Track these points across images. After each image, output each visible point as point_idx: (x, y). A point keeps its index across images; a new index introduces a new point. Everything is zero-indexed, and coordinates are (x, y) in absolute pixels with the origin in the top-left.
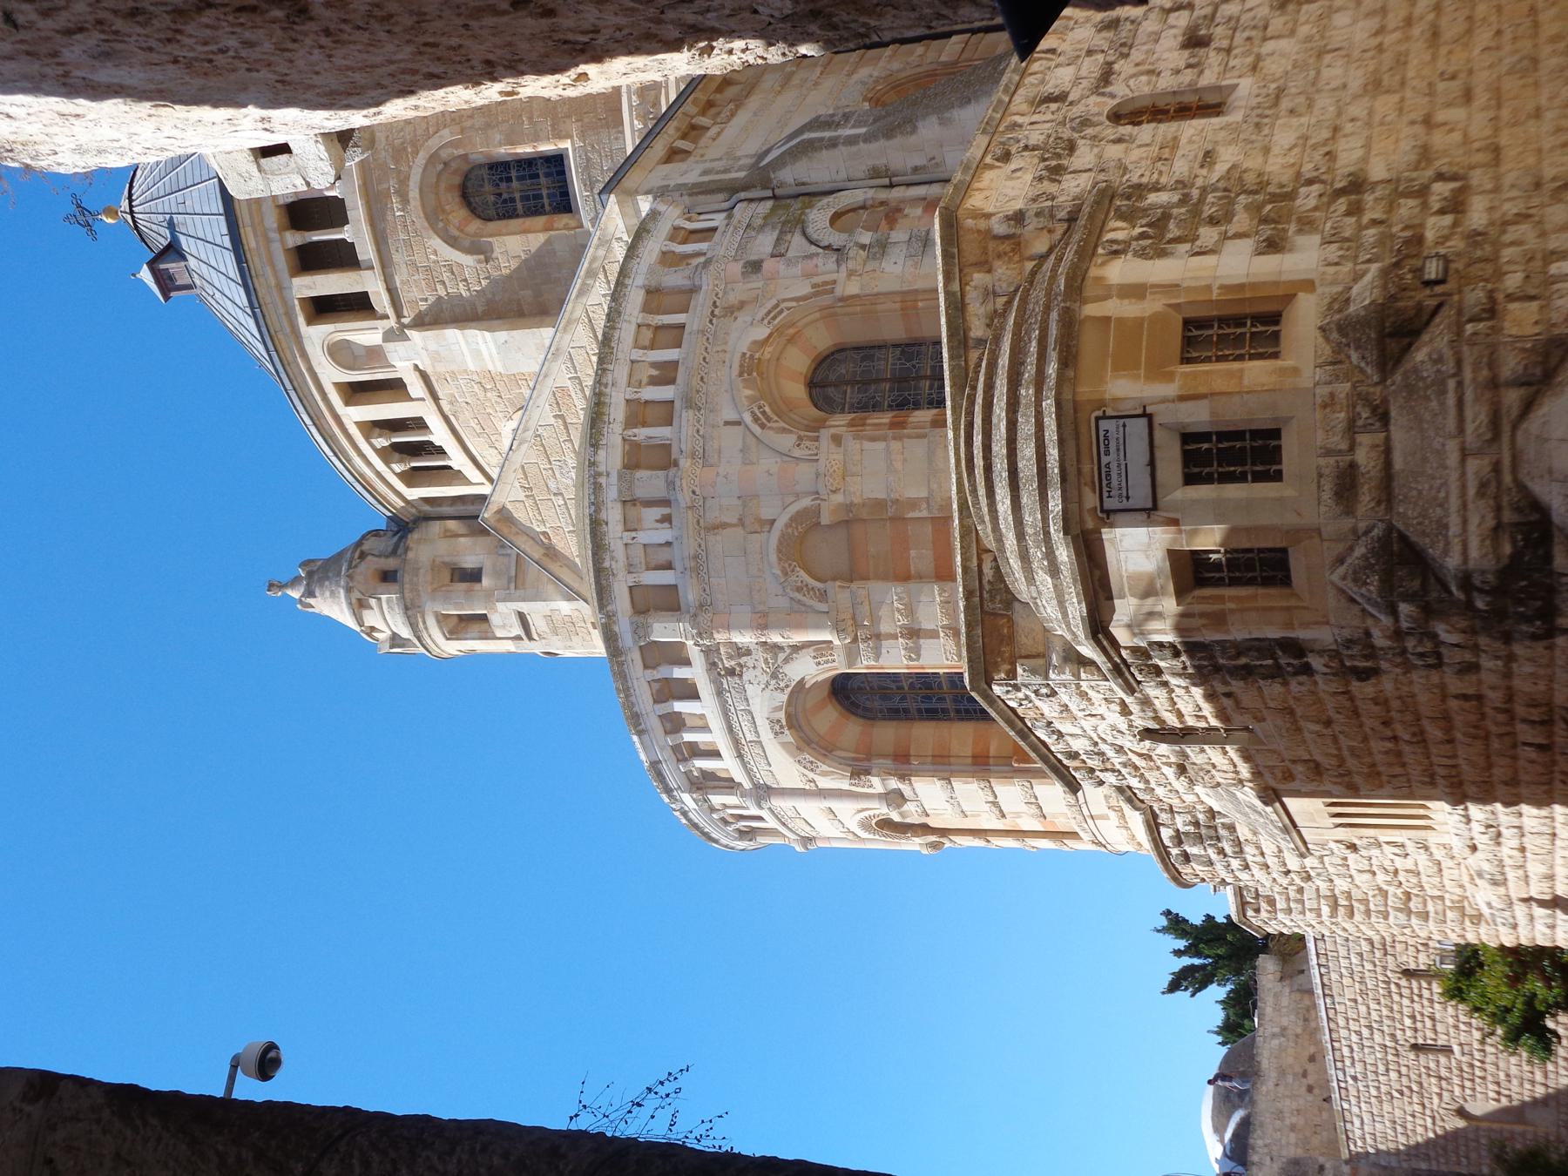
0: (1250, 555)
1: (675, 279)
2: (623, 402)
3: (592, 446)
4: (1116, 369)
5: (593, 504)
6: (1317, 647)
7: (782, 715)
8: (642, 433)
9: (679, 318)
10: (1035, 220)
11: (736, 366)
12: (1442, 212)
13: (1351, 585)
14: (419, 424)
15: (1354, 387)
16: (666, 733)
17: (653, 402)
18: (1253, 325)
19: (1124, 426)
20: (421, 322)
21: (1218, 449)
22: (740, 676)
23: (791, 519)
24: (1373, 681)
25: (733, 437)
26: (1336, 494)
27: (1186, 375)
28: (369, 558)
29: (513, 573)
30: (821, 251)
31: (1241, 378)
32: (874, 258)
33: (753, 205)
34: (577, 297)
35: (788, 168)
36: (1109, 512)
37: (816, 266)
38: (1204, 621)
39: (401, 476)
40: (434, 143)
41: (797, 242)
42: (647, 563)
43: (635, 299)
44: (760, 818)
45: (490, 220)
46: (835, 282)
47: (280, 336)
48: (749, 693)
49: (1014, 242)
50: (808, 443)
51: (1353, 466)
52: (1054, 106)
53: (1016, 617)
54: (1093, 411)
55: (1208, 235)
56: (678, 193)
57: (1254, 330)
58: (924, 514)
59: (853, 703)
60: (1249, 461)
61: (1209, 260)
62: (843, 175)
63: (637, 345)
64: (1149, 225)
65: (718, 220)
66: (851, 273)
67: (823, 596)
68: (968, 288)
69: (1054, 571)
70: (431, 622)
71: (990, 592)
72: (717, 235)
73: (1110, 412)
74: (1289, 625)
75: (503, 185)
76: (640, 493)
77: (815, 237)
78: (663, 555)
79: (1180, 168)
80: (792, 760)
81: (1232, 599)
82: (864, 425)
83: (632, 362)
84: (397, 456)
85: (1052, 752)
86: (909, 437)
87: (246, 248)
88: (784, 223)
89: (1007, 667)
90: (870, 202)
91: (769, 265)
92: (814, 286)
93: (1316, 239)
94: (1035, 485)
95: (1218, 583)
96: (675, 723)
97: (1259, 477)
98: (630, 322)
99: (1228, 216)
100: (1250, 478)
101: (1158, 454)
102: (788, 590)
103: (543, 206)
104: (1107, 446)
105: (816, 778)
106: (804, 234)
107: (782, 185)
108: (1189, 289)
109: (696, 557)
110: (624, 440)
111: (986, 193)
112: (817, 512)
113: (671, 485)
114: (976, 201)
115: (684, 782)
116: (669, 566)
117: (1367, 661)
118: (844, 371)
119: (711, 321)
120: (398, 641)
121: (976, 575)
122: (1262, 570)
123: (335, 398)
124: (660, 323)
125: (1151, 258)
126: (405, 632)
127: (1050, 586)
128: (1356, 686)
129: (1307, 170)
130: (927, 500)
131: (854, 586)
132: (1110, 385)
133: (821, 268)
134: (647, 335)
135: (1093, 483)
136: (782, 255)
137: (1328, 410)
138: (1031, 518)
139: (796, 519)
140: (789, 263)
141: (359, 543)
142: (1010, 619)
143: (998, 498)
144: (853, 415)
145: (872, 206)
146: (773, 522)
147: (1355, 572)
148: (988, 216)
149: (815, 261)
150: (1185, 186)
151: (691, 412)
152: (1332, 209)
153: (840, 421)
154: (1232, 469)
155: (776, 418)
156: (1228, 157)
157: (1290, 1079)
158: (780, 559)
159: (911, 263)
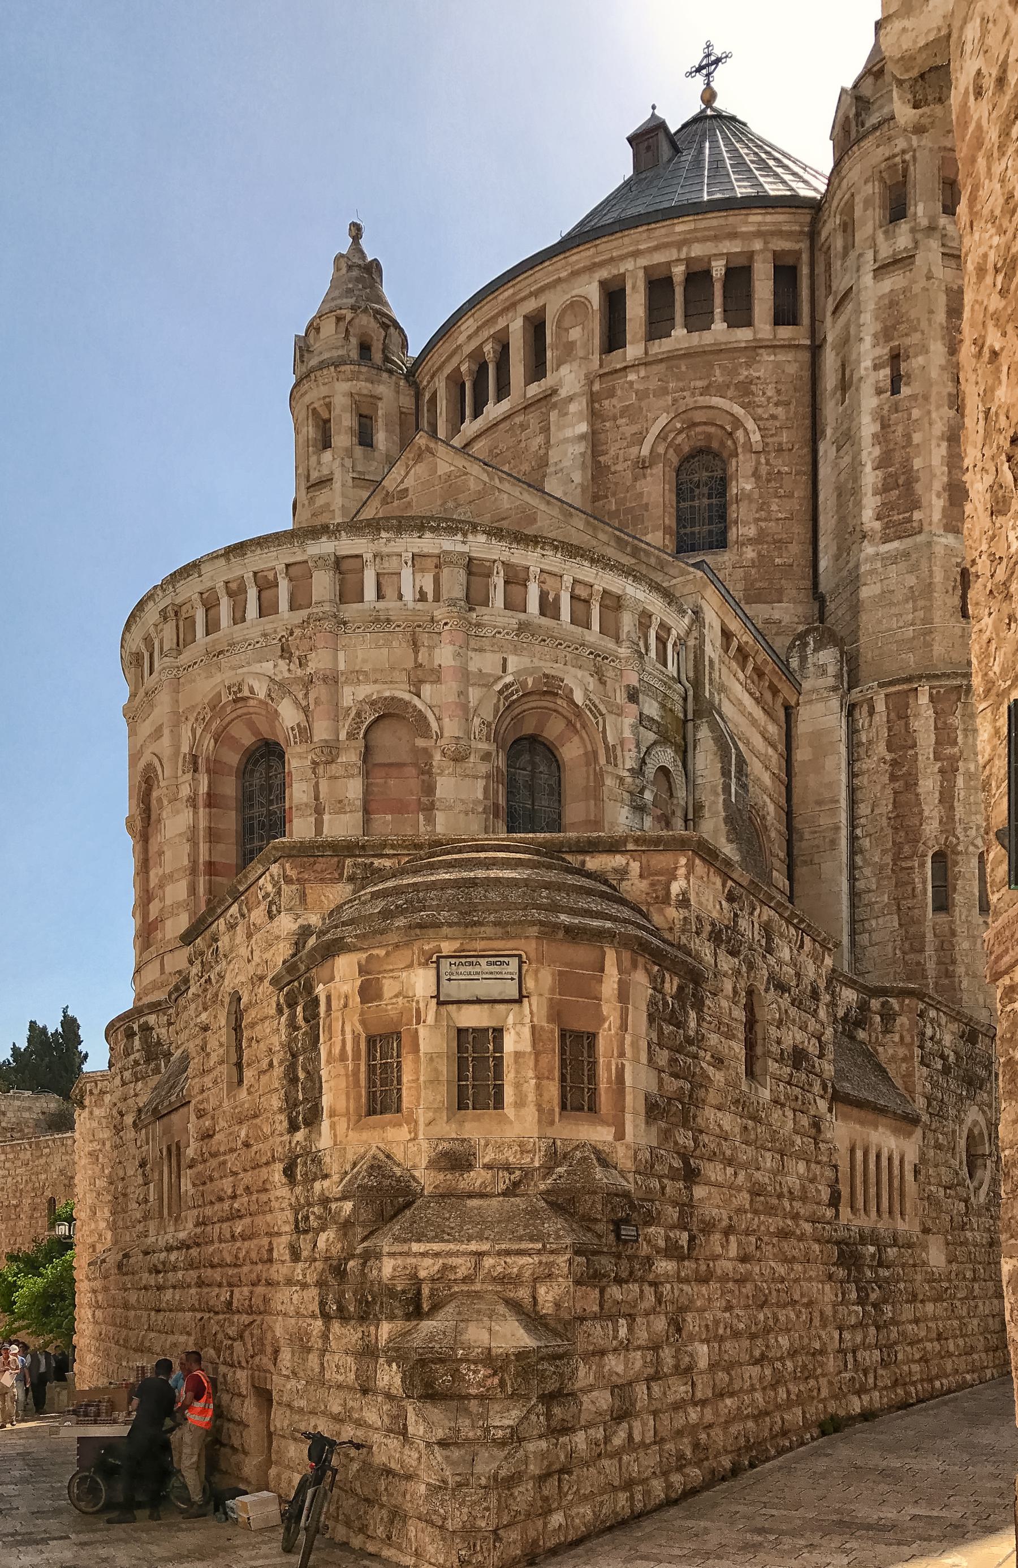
1: (628, 621)
7: (246, 693)
9: (596, 626)
11: (553, 672)
12: (667, 1238)
20: (593, 398)
22: (281, 657)
24: (284, 1180)
40: (750, 425)
48: (265, 664)
52: (763, 942)
73: (525, 967)
79: (713, 1039)
101: (486, 1006)
104: (495, 963)
119: (591, 653)
128: (279, 1167)
129: (705, 1138)
150: (699, 1041)
156: (718, 1077)
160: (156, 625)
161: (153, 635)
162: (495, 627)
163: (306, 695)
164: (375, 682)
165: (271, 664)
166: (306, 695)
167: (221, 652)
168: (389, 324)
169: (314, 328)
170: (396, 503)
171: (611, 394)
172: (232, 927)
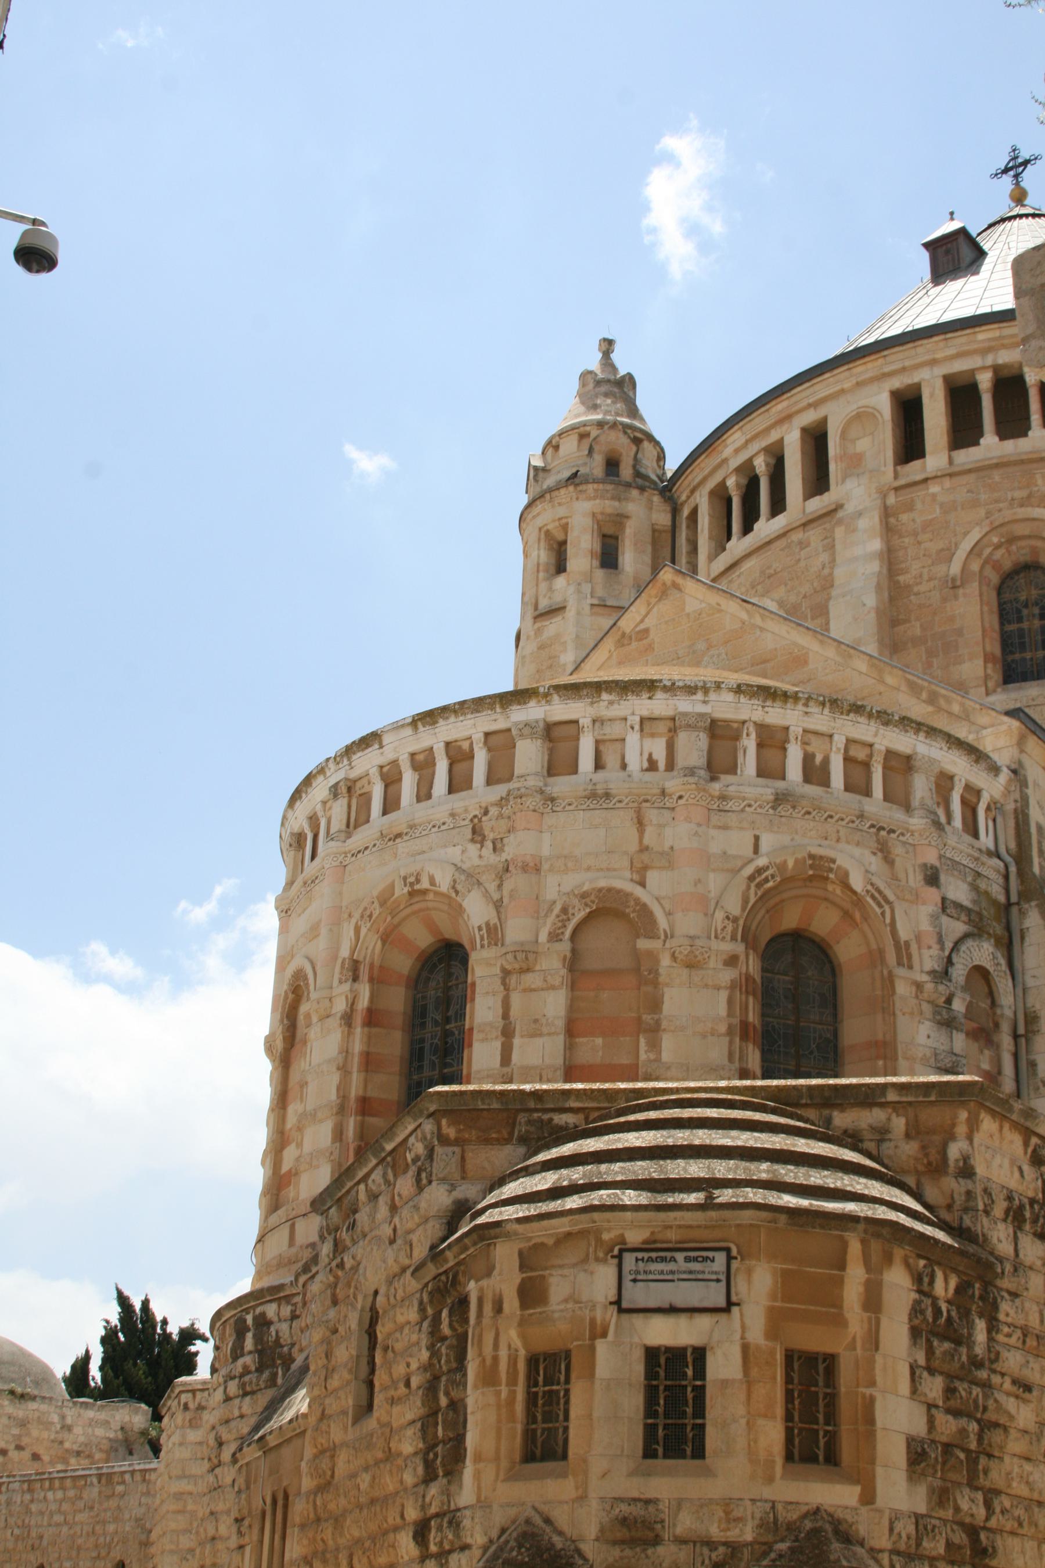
0: (561, 1417)
1: (921, 787)
2: (786, 723)
3: (739, 686)
4: (786, 1274)
5: (673, 684)
6: (453, 1488)
7: (425, 884)
8: (749, 743)
10: (963, 1190)
13: (520, 1530)
14: (778, 506)
15: (746, 1544)
16: (413, 755)
17: (785, 757)
18: (826, 1432)
19: (718, 1281)
20: (887, 513)
21: (686, 1386)
22: (473, 840)
23: (645, 905)
25: (738, 843)
26: (625, 1519)
27: (772, 1353)
28: (634, 448)
29: (609, 603)
30: (947, 953)
31: (765, 1416)
32: (936, 1013)
33: (1001, 881)
34: (908, 681)
36: (620, 1257)
37: (930, 947)
38: (489, 1362)
39: (722, 485)
41: (957, 927)
42: (604, 741)
43: (902, 742)
44: (313, 856)
45: (999, 594)
46: (910, 967)
47: (881, 361)
49: (938, 1168)
50: (730, 928)
51: (657, 1541)
53: (508, 1149)
54: (738, 1246)
55: (934, 1387)
56: (1017, 796)
57: (821, 1433)
58: (643, 1056)
59: (435, 966)
60: (670, 1421)
61: (905, 1387)
62: (1030, 982)
63: (850, 742)
64: (949, 1318)
65: (986, 840)
66: (919, 986)
67: (555, 937)
68: (890, 1110)
69: (556, 1193)
70: (561, 512)
71: (542, 1121)
72: (968, 838)
73: (735, 1264)
74: (478, 1458)
75: (1036, 611)
76: (683, 738)
77: (963, 948)
78: (611, 760)
80: (375, 893)
81: (512, 1394)
82: (747, 992)
83: (831, 736)
84: (744, 482)
85: (358, 1183)
86: (731, 1043)
87: (977, 329)
88: (979, 914)
89: (451, 1132)
90: (999, 1011)
91: (933, 895)
92: (907, 944)
93: (922, 1509)
94: (655, 1175)
95: (531, 1380)
96: (423, 764)
97: (650, 1432)
98: (876, 735)
99: (956, 1413)
100: (650, 1421)
101: (683, 1320)
102: (565, 898)
103: (1012, 653)
104: (695, 1259)
105: (354, 921)
106: (966, 936)
107: (1022, 913)
108: (871, 1362)
109: (607, 795)
110: (744, 722)
111: (997, 1135)
112: (652, 934)
113: (691, 772)
114: (988, 1124)
115: (354, 774)
116: (599, 765)
117: (435, 1544)
118: (810, 973)
119: (872, 826)
120: (541, 474)
121: (560, 1105)
122: (544, 1430)
123: (809, 418)
124: (873, 769)
125: (910, 1320)
126: (550, 481)
127: (540, 1188)
130: (658, 1060)
131: (564, 972)
133: (926, 953)
134: (860, 754)
136: (944, 909)
137: (722, 1514)
138: (616, 1170)
139: (645, 911)
140: (934, 918)
141: (650, 438)
142: (508, 1141)
143: (644, 1133)
144: (758, 980)
145: (995, 1014)
146: (643, 884)
147: (533, 1535)
148: (970, 1138)
149: (936, 946)
150: (992, 1362)
151: (772, 798)
152: (955, 1527)
153: (753, 966)
154: (662, 1402)
155: (759, 893)
157: (16, 1431)
158: (600, 890)
159: (928, 1054)
160: (324, 803)
161: (320, 814)
162: (744, 799)
163: (500, 887)
164: (588, 869)
165: (458, 850)
166: (500, 887)
167: (399, 835)
168: (642, 438)
169: (552, 445)
170: (634, 645)
171: (910, 507)
172: (374, 1197)
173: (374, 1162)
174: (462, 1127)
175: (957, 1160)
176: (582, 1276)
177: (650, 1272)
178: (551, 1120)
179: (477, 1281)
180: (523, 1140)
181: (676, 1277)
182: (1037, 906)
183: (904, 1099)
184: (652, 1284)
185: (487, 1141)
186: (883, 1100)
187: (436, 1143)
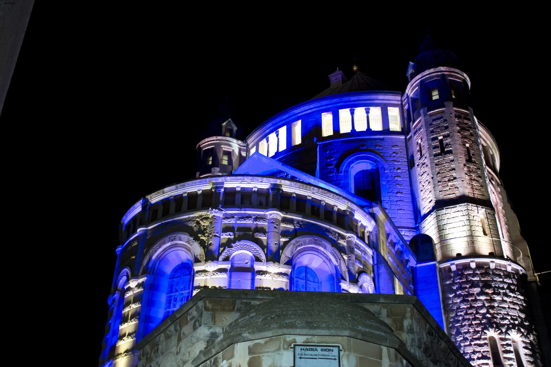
10: (411, 338)
19: (335, 359)
35: (385, 271)
36: (294, 348)
68: (381, 306)
73: (342, 353)
104: (325, 350)
121: (254, 297)
132: (354, 354)
135: (308, 342)
142: (232, 310)
173: (170, 323)
174: (214, 304)
175: (407, 326)
176: (277, 356)
177: (307, 355)
178: (250, 303)
179: (227, 361)
180: (239, 310)
181: (317, 357)
182: (384, 266)
183: (387, 302)
184: (307, 360)
185: (224, 310)
186: (378, 302)
187: (204, 310)
